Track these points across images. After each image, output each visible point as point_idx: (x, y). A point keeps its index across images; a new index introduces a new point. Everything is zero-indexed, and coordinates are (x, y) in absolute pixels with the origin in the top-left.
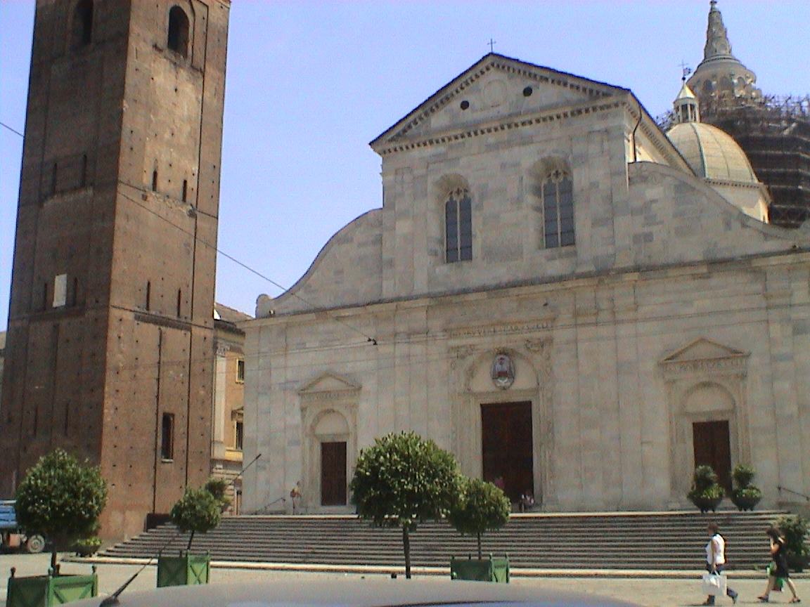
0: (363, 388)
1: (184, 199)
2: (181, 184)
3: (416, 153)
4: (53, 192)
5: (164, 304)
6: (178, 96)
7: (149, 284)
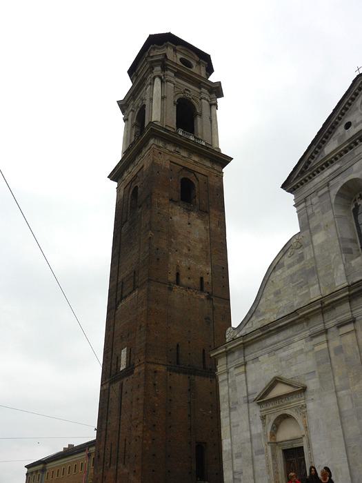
0: (309, 389)
1: (202, 289)
2: (199, 280)
3: (317, 180)
6: (191, 227)
7: (178, 345)
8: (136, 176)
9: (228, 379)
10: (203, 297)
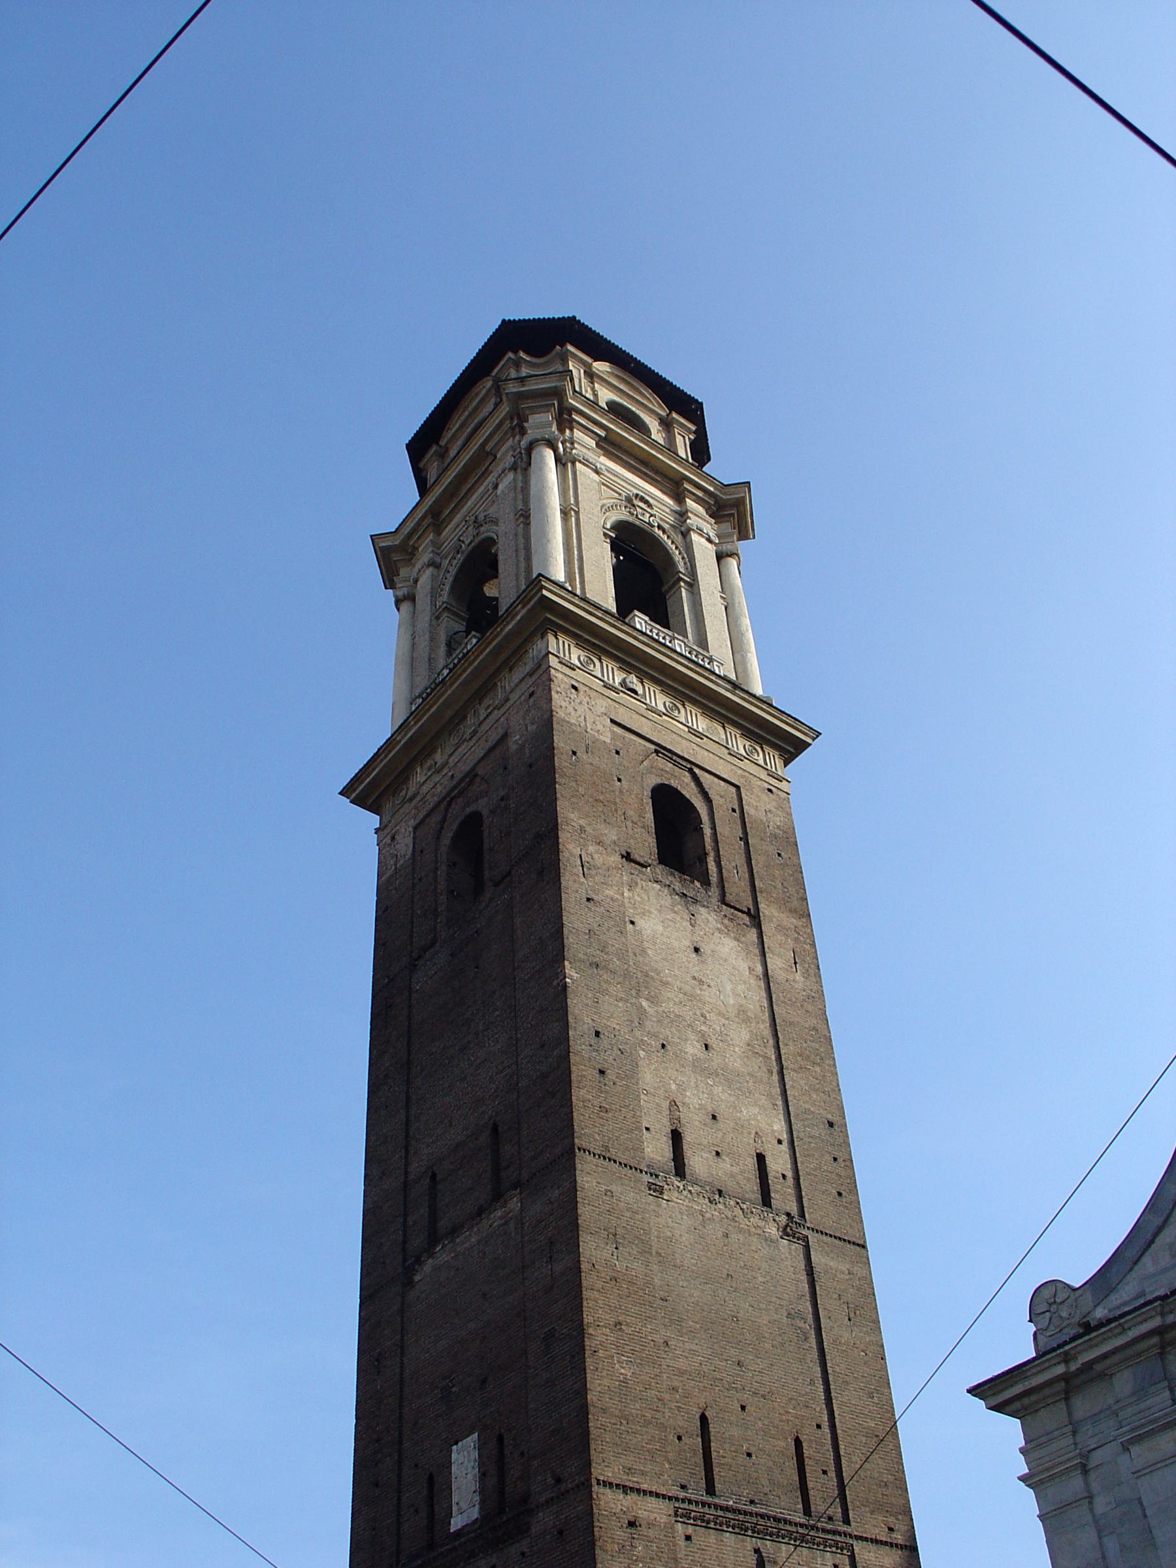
1: (766, 1201)
2: (752, 1163)
4: (434, 1239)
5: (756, 1468)
7: (704, 1419)
8: (472, 775)
9: (1090, 1498)
10: (773, 1231)
